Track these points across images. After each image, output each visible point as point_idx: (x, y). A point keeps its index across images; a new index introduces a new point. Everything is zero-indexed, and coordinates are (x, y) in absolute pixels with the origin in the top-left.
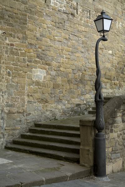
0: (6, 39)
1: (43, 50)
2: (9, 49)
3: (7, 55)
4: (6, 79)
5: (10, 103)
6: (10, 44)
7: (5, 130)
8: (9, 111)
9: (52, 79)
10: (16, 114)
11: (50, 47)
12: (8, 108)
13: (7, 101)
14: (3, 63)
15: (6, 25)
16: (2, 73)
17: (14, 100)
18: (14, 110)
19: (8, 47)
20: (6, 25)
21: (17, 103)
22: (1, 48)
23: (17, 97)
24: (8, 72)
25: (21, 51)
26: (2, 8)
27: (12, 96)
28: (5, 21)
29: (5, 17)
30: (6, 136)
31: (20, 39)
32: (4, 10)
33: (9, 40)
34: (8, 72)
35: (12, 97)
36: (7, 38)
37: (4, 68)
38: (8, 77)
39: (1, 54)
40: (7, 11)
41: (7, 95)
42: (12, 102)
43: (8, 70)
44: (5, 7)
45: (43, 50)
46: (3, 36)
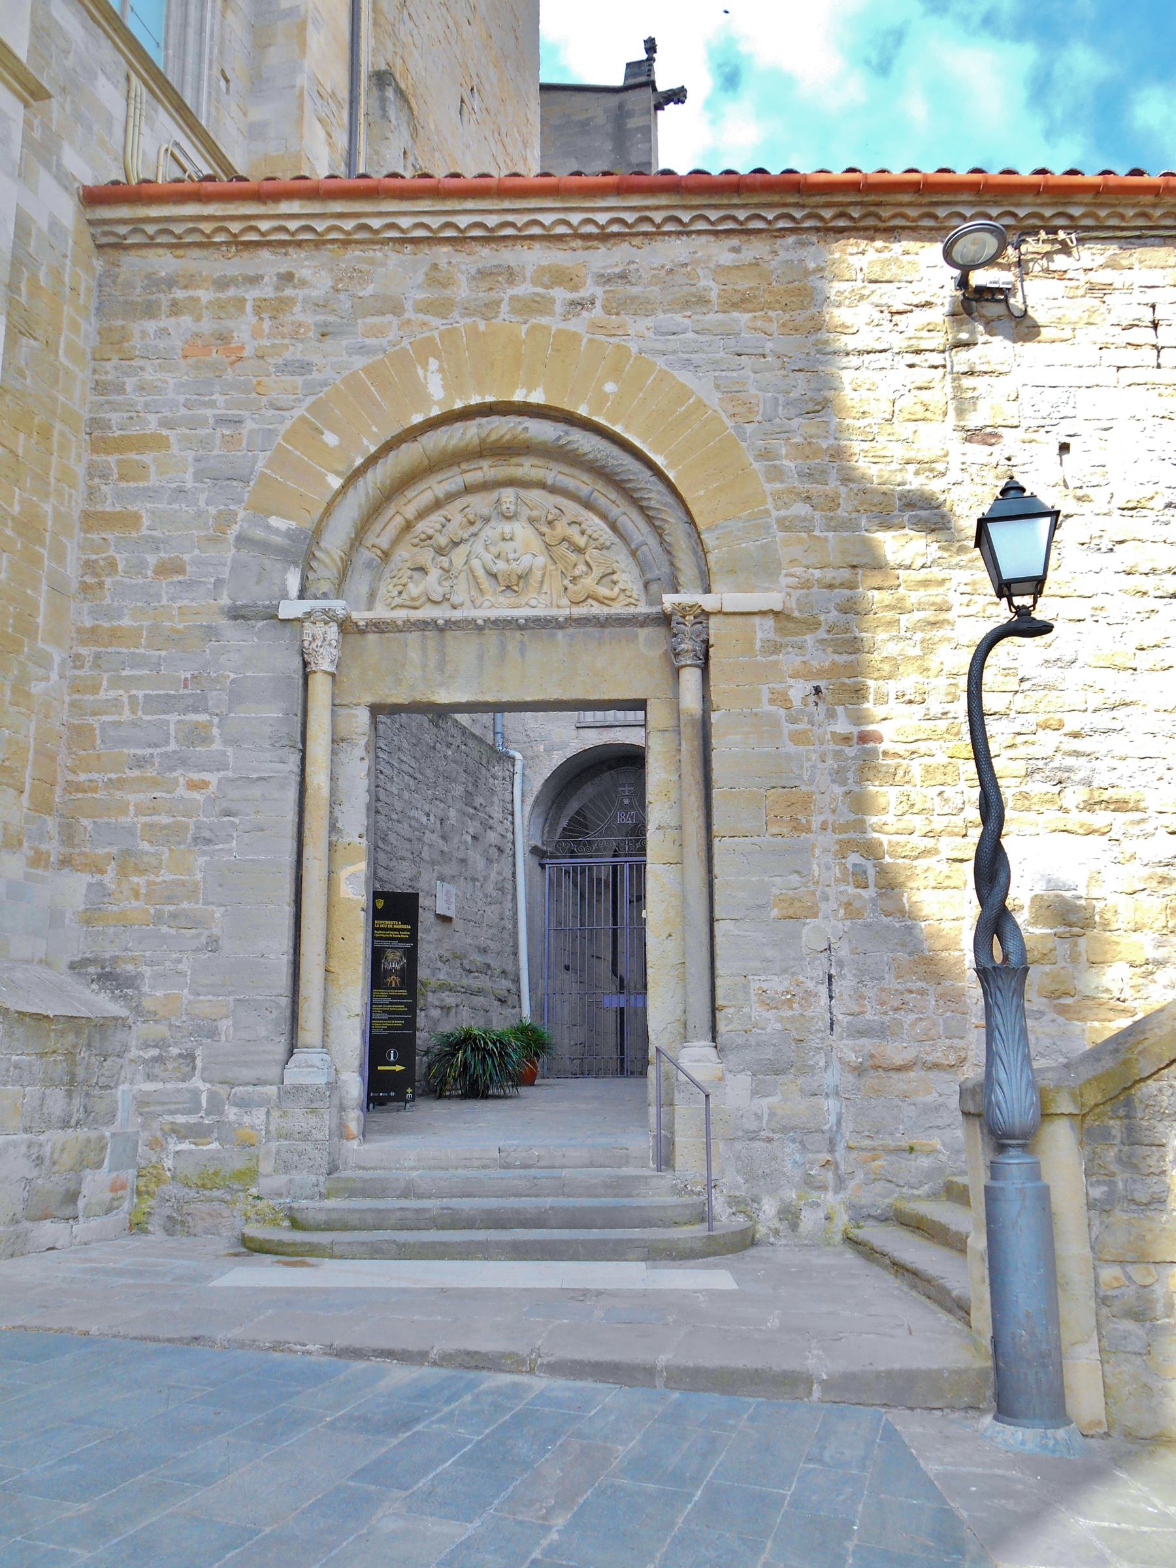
0: (831, 715)
1: (1075, 735)
2: (853, 758)
3: (838, 790)
4: (845, 899)
5: (868, 1016)
6: (855, 734)
7: (850, 1148)
8: (872, 1056)
9: (1154, 884)
10: (912, 1074)
11: (1121, 713)
12: (864, 1041)
13: (856, 1009)
14: (824, 827)
15: (830, 650)
16: (816, 873)
17: (896, 1004)
18: (896, 1051)
19: (847, 750)
20: (830, 650)
21: (912, 1017)
22: (809, 760)
23: (909, 985)
24: (849, 866)
25: (926, 760)
26: (803, 580)
27: (885, 984)
28: (826, 636)
29: (822, 618)
30: (852, 1184)
31: (910, 702)
32: (815, 590)
33: (848, 716)
34: (849, 866)
35: (882, 990)
36: (840, 709)
37: (826, 850)
38: (851, 890)
39: (813, 788)
40: (830, 586)
41: (849, 977)
42: (885, 1013)
43: (854, 858)
44: (817, 573)
45: (1075, 735)
46: (817, 704)
